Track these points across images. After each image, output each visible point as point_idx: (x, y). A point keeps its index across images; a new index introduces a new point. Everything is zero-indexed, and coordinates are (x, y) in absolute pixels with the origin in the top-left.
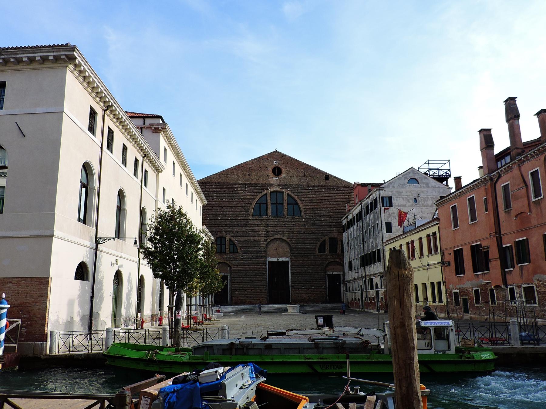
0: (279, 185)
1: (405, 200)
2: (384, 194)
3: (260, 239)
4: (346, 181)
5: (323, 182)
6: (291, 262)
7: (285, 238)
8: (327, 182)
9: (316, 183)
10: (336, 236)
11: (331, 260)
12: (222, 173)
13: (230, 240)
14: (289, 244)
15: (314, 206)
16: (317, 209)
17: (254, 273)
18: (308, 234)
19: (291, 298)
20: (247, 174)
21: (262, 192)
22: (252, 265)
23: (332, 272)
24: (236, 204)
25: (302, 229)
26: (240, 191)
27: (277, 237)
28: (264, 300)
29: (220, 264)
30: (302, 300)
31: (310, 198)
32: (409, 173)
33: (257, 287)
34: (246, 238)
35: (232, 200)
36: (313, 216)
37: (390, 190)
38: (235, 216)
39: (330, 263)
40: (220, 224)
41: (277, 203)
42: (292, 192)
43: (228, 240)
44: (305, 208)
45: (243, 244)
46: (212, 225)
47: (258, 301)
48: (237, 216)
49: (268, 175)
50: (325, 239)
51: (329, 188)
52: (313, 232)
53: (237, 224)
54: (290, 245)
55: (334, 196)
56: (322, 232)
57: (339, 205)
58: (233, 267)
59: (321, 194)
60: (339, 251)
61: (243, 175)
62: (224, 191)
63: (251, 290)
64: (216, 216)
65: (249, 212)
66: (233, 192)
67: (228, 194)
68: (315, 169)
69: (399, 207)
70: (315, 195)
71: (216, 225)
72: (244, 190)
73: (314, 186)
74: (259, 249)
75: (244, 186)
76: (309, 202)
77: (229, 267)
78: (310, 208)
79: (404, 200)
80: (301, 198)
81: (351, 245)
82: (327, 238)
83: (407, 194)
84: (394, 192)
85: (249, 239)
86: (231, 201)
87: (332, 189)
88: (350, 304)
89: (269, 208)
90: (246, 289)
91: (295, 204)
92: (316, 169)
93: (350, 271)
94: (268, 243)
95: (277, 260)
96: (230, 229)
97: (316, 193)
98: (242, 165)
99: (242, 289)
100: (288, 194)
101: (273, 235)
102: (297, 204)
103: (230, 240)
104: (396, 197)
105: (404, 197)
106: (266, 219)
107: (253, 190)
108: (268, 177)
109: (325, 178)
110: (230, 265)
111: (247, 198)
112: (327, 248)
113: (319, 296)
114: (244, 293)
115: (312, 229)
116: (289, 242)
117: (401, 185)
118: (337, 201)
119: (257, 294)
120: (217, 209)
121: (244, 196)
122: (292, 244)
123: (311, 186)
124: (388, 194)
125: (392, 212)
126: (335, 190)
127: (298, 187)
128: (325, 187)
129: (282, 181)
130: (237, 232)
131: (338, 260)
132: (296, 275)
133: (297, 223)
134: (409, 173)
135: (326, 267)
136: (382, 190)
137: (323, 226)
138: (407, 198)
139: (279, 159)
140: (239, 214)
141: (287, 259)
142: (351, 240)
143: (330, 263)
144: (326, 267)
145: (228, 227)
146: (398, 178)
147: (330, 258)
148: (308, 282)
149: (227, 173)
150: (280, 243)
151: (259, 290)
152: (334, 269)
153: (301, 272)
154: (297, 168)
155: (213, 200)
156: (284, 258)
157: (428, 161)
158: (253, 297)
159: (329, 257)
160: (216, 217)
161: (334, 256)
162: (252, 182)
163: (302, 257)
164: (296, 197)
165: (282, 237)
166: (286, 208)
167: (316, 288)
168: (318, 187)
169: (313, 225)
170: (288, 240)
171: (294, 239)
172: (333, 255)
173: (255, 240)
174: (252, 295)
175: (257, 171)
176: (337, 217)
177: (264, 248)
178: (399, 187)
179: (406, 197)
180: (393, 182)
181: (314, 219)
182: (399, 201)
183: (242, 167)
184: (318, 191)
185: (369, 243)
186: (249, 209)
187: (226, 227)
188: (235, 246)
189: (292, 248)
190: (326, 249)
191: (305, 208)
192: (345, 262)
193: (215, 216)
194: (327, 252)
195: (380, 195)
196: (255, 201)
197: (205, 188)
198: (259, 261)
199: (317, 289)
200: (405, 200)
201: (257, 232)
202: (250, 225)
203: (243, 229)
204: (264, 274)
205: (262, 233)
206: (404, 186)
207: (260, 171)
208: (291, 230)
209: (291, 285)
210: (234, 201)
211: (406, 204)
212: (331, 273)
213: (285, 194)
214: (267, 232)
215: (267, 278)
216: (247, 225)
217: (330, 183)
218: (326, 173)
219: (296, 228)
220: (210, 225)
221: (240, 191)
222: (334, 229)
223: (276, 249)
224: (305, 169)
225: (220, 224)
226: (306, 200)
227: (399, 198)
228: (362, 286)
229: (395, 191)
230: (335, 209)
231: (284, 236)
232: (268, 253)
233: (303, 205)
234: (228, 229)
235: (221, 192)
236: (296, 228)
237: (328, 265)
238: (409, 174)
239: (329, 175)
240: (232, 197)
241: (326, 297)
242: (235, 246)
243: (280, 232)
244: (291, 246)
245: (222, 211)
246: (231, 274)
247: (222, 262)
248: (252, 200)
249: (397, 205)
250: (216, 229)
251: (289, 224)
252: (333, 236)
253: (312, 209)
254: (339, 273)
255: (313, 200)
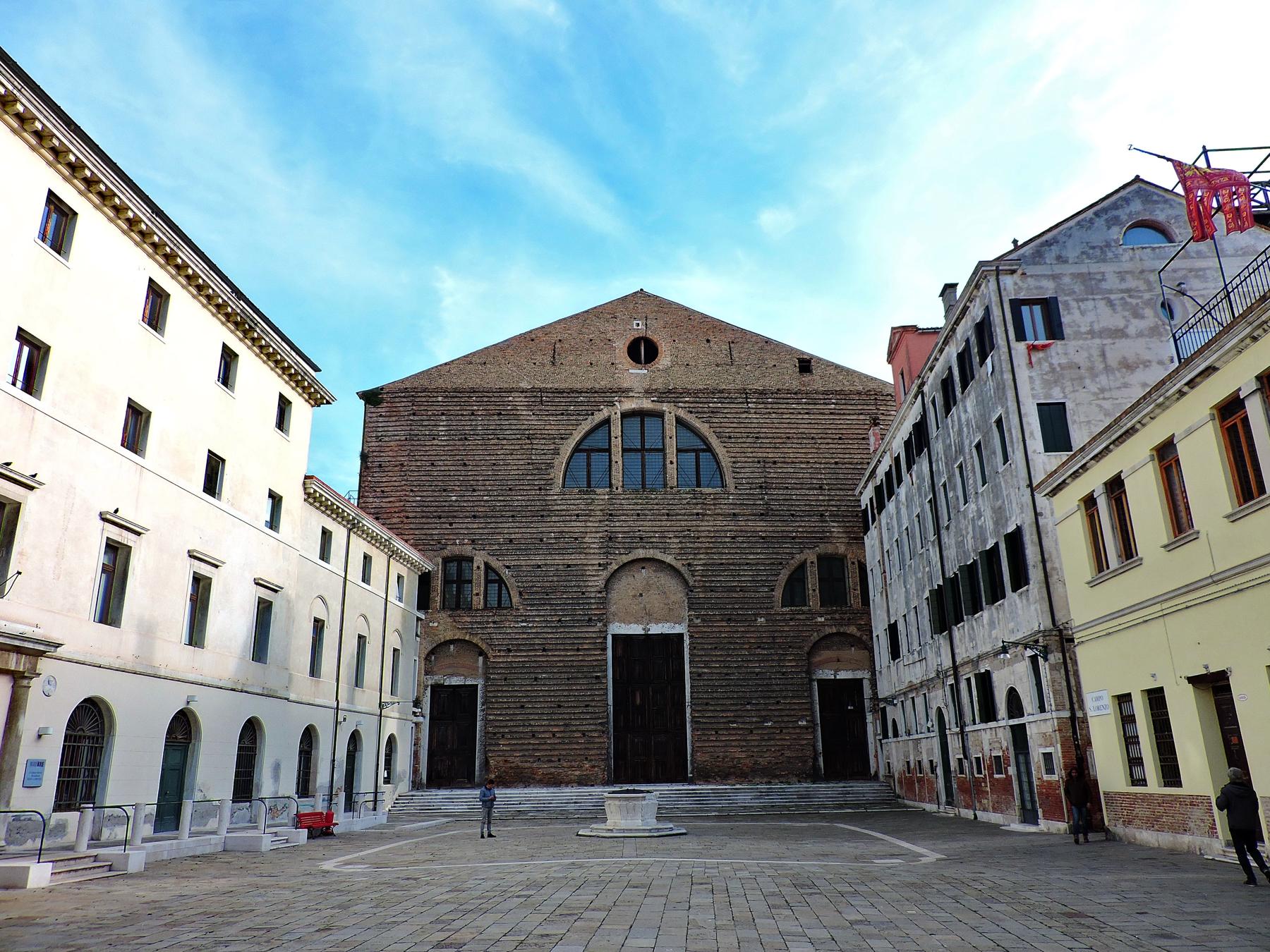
0: (648, 392)
1: (1119, 308)
2: (1020, 288)
3: (585, 562)
4: (866, 376)
5: (792, 380)
6: (691, 637)
7: (669, 559)
8: (807, 378)
9: (771, 382)
10: (842, 549)
11: (828, 630)
12: (467, 360)
13: (486, 564)
14: (684, 578)
15: (765, 455)
16: (775, 463)
17: (563, 676)
18: (745, 545)
19: (691, 760)
20: (548, 359)
21: (592, 414)
22: (556, 650)
23: (833, 672)
24: (508, 452)
25: (726, 528)
26: (524, 413)
27: (641, 556)
28: (596, 769)
29: (452, 647)
30: (732, 770)
31: (751, 430)
32: (1126, 200)
33: (573, 722)
34: (538, 560)
35: (498, 439)
36: (761, 487)
37: (1050, 273)
38: (504, 487)
39: (826, 641)
40: (455, 514)
41: (643, 450)
42: (691, 412)
43: (478, 568)
44: (734, 459)
45: (530, 579)
46: (428, 517)
47: (577, 773)
48: (510, 489)
49: (613, 364)
50: (806, 559)
51: (812, 397)
52: (763, 538)
53: (511, 513)
54: (686, 582)
55: (831, 422)
56: (794, 538)
57: (847, 451)
58: (495, 656)
59: (788, 416)
60: (854, 600)
61: (535, 364)
62: (473, 414)
63: (554, 735)
64: (445, 490)
65: (552, 476)
66: (500, 414)
67: (486, 422)
68: (767, 342)
69: (1093, 338)
70: (768, 421)
71: (443, 520)
72: (536, 408)
73: (762, 393)
74: (583, 593)
75: (537, 396)
76: (749, 440)
77: (480, 655)
78: (750, 460)
79: (1114, 310)
80: (721, 430)
81: (894, 566)
82: (811, 556)
83: (1124, 286)
84: (1067, 280)
85: (548, 562)
86: (492, 442)
87: (822, 402)
88: (900, 782)
89: (616, 462)
90: (535, 729)
91: (704, 451)
92: (768, 341)
93: (894, 659)
94: (614, 574)
95: (643, 632)
96: (486, 531)
97: (770, 413)
98: (534, 336)
99: (521, 729)
100: (679, 421)
101: (630, 549)
102: (709, 449)
103: (486, 564)
104: (1077, 301)
105: (1113, 297)
106: (607, 497)
107: (565, 408)
108: (613, 369)
109: (800, 367)
110: (484, 647)
111: (546, 432)
112: (814, 590)
113: (788, 753)
114: (530, 744)
115: (760, 526)
116: (683, 570)
117: (1093, 248)
118: (840, 438)
119: (571, 750)
120: (447, 468)
121: (536, 427)
122: (694, 576)
123: (754, 393)
124: (1041, 288)
125: (1064, 361)
126: (833, 403)
127: (712, 396)
128: (800, 396)
129: (661, 380)
130: (511, 541)
131: (852, 630)
132: (706, 683)
133: (709, 510)
134: (1126, 200)
135: (810, 654)
136: (1013, 272)
137: (798, 519)
138: (1129, 300)
139: (650, 316)
140: (517, 482)
141: (678, 629)
142: (892, 546)
143: (826, 641)
144: (810, 654)
145: (481, 526)
146: (1078, 223)
147: (823, 625)
148: (749, 707)
149: (483, 360)
150: (653, 574)
151: (579, 735)
152: (838, 661)
153: (725, 671)
154: (708, 341)
155: (435, 442)
156: (666, 625)
157: (1205, 151)
158: (559, 760)
159: (819, 619)
160: (444, 494)
161: (837, 616)
162: (563, 386)
163: (729, 620)
164: (704, 428)
165: (659, 554)
166: (672, 463)
167: (777, 726)
168: (778, 396)
169: (762, 514)
170: (678, 565)
171: (700, 559)
172: (835, 612)
173: (569, 566)
174: (556, 753)
175: (579, 353)
176: (842, 487)
177: (600, 592)
178: (1089, 258)
179: (1122, 298)
180: (1055, 241)
181: (766, 494)
182: (1091, 317)
183: (533, 340)
184: (775, 406)
185: (963, 523)
186: (550, 466)
187: (475, 526)
188: (504, 588)
189: (692, 591)
190: (810, 592)
191: (734, 462)
192: (874, 635)
193: (439, 491)
194: (814, 601)
195: (1003, 293)
196: (569, 441)
197: (413, 405)
198: (582, 635)
199: (781, 731)
200: (1119, 308)
201: (576, 539)
202: (554, 519)
203: (528, 530)
204: (597, 677)
205: (592, 541)
206: (1110, 255)
207: (588, 350)
208: (689, 530)
209: (693, 717)
210: (505, 442)
211: (1126, 327)
212: (827, 674)
213: (670, 421)
214: (610, 538)
215: (606, 694)
216: (542, 516)
217: (815, 382)
218: (803, 353)
219: (706, 525)
220: (423, 517)
221: (524, 413)
222: (834, 527)
223: (641, 595)
224: (733, 342)
225: (455, 517)
226: (739, 435)
227: (1090, 304)
228: (944, 711)
229: (1071, 274)
230: (836, 463)
231: (665, 550)
232: (613, 609)
233: (727, 452)
234: (481, 531)
235: (462, 415)
236: (707, 524)
237: (816, 647)
238: (1128, 204)
239: (812, 357)
240: (498, 432)
241: (815, 759)
242: (504, 588)
243: (654, 540)
244: (691, 583)
245: (463, 473)
246: (487, 679)
247: (458, 640)
248: (562, 438)
249: (1083, 329)
250: (442, 531)
251: (683, 511)
252: (830, 549)
253: (759, 462)
254: (859, 675)
255: (762, 435)
